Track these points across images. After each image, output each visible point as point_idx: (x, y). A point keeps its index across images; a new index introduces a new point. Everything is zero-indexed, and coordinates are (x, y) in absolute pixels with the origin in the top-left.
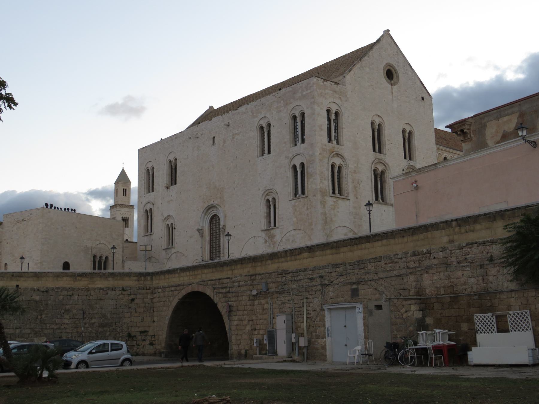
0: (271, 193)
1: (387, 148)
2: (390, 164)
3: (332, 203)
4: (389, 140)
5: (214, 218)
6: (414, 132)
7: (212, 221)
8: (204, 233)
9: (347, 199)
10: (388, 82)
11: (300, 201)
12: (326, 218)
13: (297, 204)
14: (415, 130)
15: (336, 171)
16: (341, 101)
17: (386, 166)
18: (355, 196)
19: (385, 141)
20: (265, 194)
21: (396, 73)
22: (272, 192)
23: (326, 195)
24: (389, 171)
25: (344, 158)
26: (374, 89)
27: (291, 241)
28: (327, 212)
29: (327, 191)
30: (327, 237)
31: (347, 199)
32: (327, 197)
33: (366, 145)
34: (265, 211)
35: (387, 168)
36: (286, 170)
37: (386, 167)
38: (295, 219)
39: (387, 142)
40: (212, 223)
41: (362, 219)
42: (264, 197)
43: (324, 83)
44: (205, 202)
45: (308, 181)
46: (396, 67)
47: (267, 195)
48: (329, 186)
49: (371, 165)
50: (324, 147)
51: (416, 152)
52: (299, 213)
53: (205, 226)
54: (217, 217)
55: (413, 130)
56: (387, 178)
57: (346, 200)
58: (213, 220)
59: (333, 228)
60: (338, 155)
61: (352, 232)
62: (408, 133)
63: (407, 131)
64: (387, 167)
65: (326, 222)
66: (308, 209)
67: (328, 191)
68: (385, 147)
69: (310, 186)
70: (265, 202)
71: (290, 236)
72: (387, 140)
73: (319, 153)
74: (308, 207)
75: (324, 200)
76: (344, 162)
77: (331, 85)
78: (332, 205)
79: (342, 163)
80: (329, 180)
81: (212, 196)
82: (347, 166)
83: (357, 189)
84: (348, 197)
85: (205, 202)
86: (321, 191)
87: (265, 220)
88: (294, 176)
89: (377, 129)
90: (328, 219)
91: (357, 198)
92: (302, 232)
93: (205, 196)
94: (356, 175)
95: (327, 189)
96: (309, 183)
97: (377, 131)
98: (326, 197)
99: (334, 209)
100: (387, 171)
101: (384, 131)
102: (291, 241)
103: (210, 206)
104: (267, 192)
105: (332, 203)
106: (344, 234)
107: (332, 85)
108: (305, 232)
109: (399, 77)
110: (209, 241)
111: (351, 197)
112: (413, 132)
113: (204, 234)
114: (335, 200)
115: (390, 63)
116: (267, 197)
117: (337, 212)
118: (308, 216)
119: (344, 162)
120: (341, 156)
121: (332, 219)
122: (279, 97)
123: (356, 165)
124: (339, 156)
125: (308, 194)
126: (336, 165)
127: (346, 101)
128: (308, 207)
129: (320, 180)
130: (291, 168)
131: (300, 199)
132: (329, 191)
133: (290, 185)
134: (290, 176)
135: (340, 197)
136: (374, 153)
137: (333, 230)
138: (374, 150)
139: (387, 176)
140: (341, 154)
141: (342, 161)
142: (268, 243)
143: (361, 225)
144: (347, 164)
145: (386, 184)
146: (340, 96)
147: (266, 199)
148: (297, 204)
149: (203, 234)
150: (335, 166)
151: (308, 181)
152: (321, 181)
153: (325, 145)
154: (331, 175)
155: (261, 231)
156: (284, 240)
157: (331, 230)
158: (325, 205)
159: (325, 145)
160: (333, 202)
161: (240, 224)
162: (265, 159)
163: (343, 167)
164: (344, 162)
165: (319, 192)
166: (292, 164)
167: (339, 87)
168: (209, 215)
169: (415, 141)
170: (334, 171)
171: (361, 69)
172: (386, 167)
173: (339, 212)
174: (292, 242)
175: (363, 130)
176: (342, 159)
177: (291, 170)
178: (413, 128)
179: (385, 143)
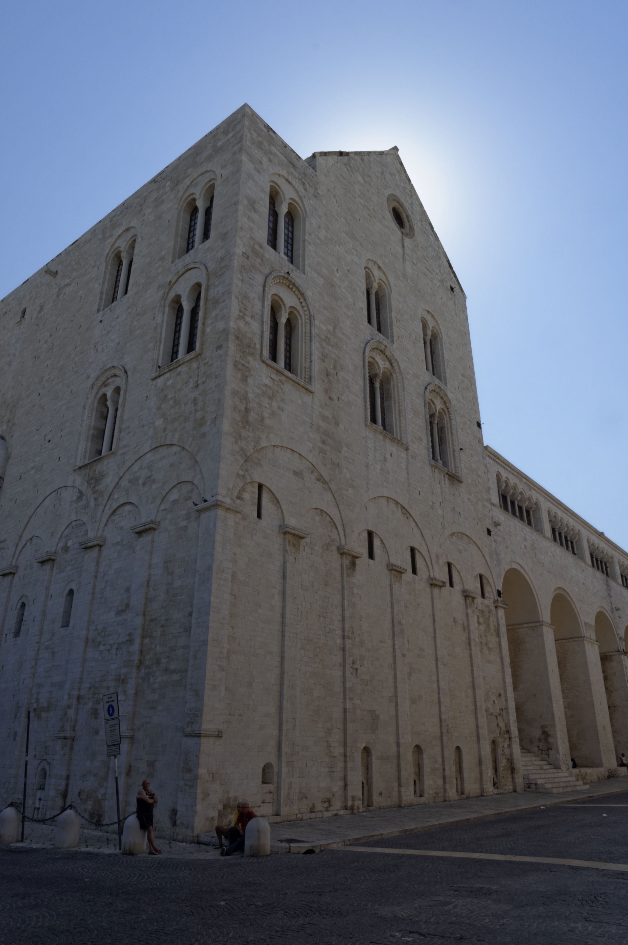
0: (114, 379)
1: (395, 331)
3: (267, 381)
4: (399, 321)
6: (441, 333)
9: (306, 389)
11: (179, 374)
12: (247, 410)
13: (169, 383)
14: (443, 332)
15: (283, 320)
16: (305, 190)
17: (394, 364)
18: (326, 391)
19: (391, 318)
20: (100, 382)
21: (409, 221)
22: (115, 376)
23: (252, 354)
24: (399, 378)
25: (305, 300)
27: (140, 482)
28: (251, 396)
29: (255, 344)
30: (246, 461)
31: (306, 389)
32: (254, 360)
33: (354, 304)
34: (92, 424)
35: (395, 370)
36: (154, 314)
37: (391, 364)
38: (159, 422)
39: (394, 320)
41: (340, 452)
42: (95, 391)
45: (205, 318)
46: (410, 212)
47: (102, 385)
48: (262, 337)
49: (363, 346)
50: (257, 247)
51: (446, 369)
52: (171, 402)
55: (438, 330)
56: (394, 388)
57: (304, 390)
59: (264, 444)
60: (292, 286)
61: (316, 474)
63: (429, 327)
64: (396, 368)
65: (246, 422)
66: (197, 386)
67: (258, 346)
68: (392, 329)
69: (208, 330)
70: (96, 404)
71: (141, 468)
72: (396, 318)
73: (243, 253)
74: (197, 381)
75: (246, 365)
76: (303, 307)
78: (266, 385)
79: (299, 307)
80: (262, 322)
82: (311, 318)
83: (331, 378)
84: (310, 384)
86: (237, 338)
87: (89, 444)
88: (174, 326)
89: (376, 290)
90: (252, 416)
91: (330, 398)
92: (175, 449)
94: (330, 348)
95: (257, 340)
96: (209, 322)
97: (374, 293)
98: (250, 359)
99: (271, 398)
100: (394, 375)
101: (390, 299)
102: (140, 482)
104: (103, 379)
105: (267, 381)
106: (294, 471)
108: (184, 448)
109: (413, 229)
111: (317, 386)
112: (439, 333)
114: (274, 376)
115: (399, 199)
116: (104, 390)
117: (279, 408)
118: (195, 404)
119: (305, 308)
121: (262, 419)
122: (164, 179)
123: (330, 328)
124: (292, 289)
125: (201, 349)
126: (284, 304)
128: (197, 381)
129: (240, 311)
130: (167, 305)
131: (179, 369)
132: (262, 350)
133: (158, 343)
134: (162, 323)
135: (289, 374)
137: (262, 448)
138: (369, 321)
139: (394, 385)
141: (298, 302)
142: (84, 498)
143: (338, 465)
144: (312, 314)
145: (393, 401)
146: (303, 180)
147: (101, 393)
148: (169, 383)
150: (280, 307)
151: (205, 318)
152: (241, 314)
154: (268, 340)
155: (74, 470)
156: (124, 483)
157: (259, 448)
158: (247, 377)
159: (261, 247)
160: (269, 379)
161: (32, 468)
162: (112, 309)
163: (302, 319)
164: (303, 307)
165: (233, 338)
166: (172, 295)
169: (442, 350)
170: (278, 320)
173: (283, 410)
174: (144, 484)
176: (299, 299)
177: (167, 309)
178: (438, 325)
179: (392, 321)
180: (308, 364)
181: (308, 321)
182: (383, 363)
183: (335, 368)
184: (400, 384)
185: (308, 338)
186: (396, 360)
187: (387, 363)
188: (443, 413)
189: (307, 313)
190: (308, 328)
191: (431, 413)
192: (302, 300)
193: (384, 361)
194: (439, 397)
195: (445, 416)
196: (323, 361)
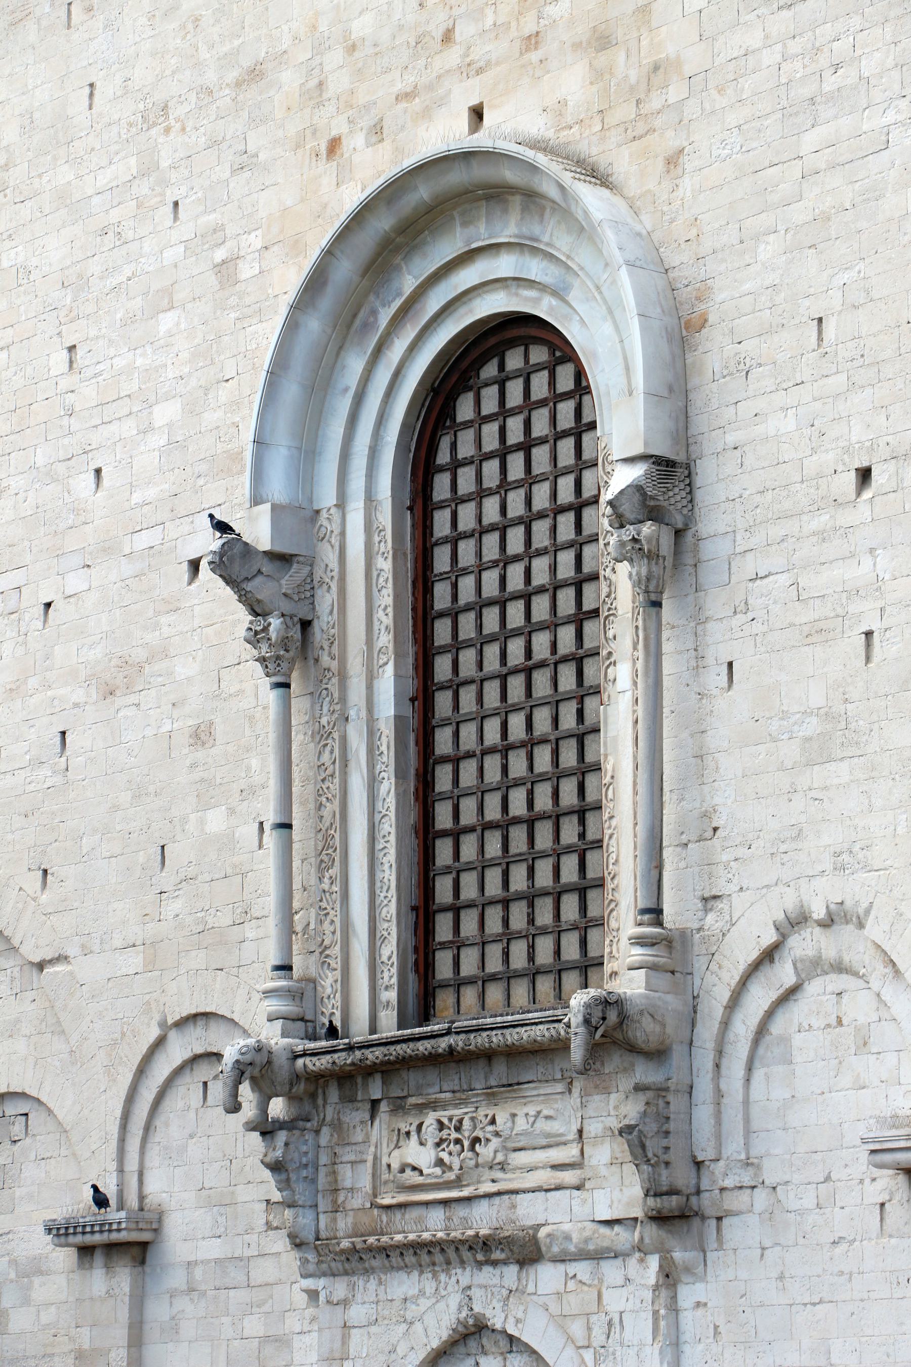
5: (490, 370)
7: (459, 427)
8: (326, 601)
40: (443, 457)
44: (334, 145)
53: (341, 504)
54: (539, 354)
58: (465, 410)
81: (448, 37)
85: (334, 145)
93: (335, 58)
103: (423, 192)
110: (399, 719)
113: (318, 634)
149: (306, 625)
168: (409, 333)
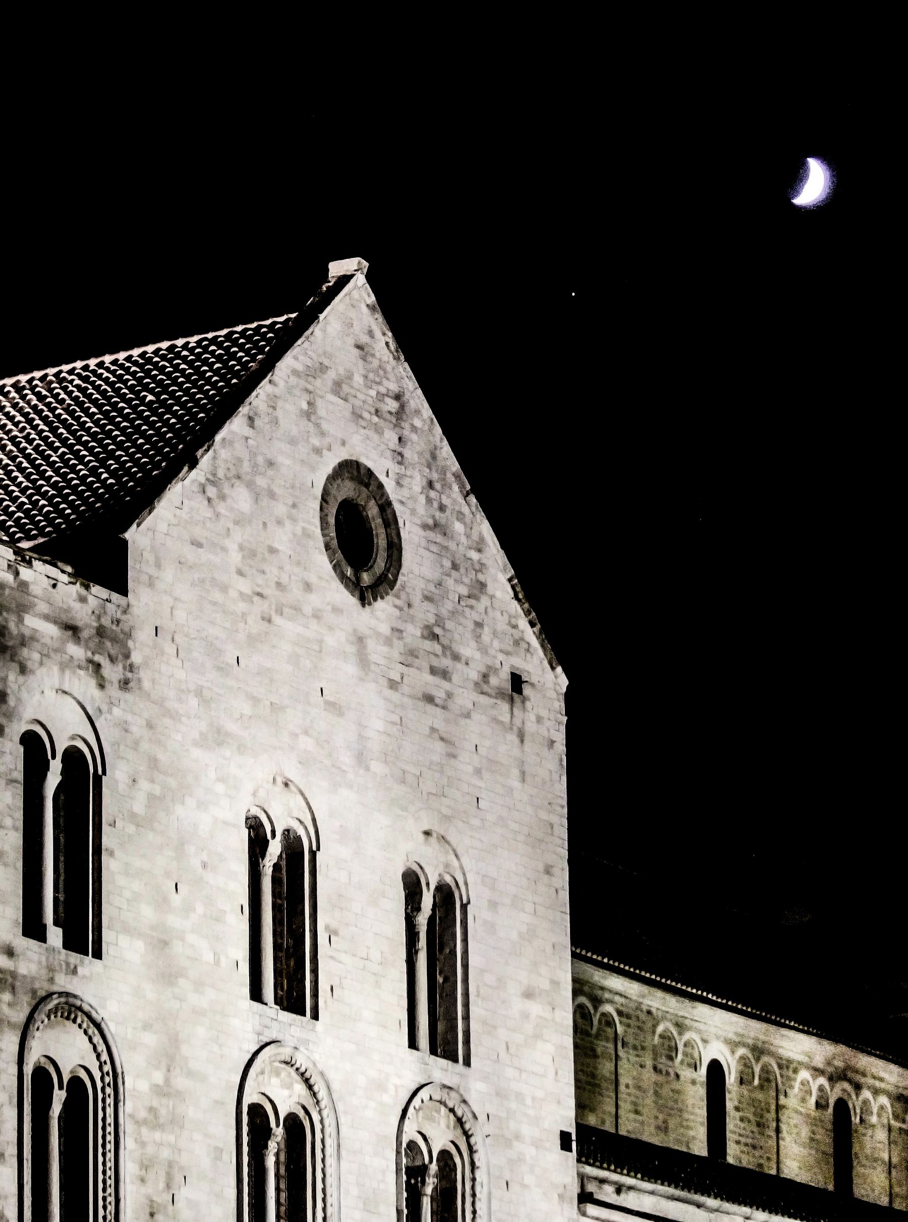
2: (331, 1076)
10: (343, 577)
17: (316, 1088)
26: (269, 621)
37: (310, 1087)
43: (17, 574)
62: (433, 887)
77: (54, 586)
107: (59, 585)
120: (98, 1026)
127: (125, 684)
136: (256, 1004)
140: (86, 1008)
146: (97, 658)
153: (10, 952)
159: (10, 952)
167: (90, 598)
171: (211, 491)
172: (310, 1087)
175: (205, 866)
180: (111, 1208)
181: (109, 1090)
182: (286, 1092)
183: (168, 1186)
184: (328, 1142)
185: (110, 1138)
186: (322, 1074)
187: (300, 1088)
188: (454, 1151)
189: (107, 1068)
190: (110, 1111)
191: (418, 1163)
192: (97, 1039)
193: (289, 1087)
194: (443, 1110)
195: (457, 1160)
196: (143, 1180)
